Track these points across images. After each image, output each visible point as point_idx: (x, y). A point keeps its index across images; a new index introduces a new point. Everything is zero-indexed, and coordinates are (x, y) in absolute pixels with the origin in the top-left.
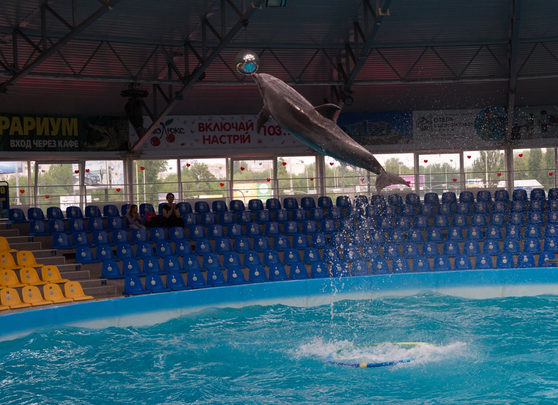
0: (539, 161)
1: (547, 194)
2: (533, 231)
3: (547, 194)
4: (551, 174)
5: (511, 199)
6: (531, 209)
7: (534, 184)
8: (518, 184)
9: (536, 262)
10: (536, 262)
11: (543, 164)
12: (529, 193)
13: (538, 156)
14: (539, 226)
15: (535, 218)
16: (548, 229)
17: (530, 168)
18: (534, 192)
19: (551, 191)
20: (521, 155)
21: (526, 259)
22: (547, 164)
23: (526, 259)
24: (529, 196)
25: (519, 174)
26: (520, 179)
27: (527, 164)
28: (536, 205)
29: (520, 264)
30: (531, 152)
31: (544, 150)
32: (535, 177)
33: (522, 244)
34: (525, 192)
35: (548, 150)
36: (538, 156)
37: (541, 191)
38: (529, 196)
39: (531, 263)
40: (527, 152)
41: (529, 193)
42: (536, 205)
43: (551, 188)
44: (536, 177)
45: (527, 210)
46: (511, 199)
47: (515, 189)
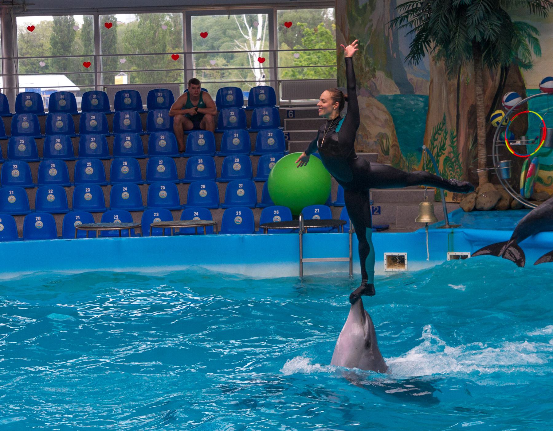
0: (71, 40)
1: (79, 100)
2: (53, 172)
3: (79, 100)
4: (87, 65)
5: (13, 111)
6: (49, 131)
7: (62, 83)
8: (26, 82)
9: (59, 229)
10: (59, 229)
11: (78, 45)
12: (45, 98)
13: (69, 32)
14: (63, 160)
15: (58, 146)
16: (80, 168)
17: (53, 53)
18: (55, 96)
19: (86, 97)
20: (31, 28)
21: (39, 223)
22: (85, 46)
23: (39, 223)
24: (46, 106)
25: (33, 64)
26: (28, 73)
27: (48, 45)
28: (59, 123)
29: (30, 233)
30: (56, 22)
31: (79, 20)
32: (62, 70)
33: (32, 194)
34: (39, 96)
35: (85, 20)
36: (69, 32)
37: (70, 96)
38: (46, 106)
39: (50, 232)
40: (48, 23)
41: (45, 98)
42: (59, 123)
43: (88, 89)
44: (65, 69)
45: (42, 130)
46: (13, 111)
47: (22, 91)
